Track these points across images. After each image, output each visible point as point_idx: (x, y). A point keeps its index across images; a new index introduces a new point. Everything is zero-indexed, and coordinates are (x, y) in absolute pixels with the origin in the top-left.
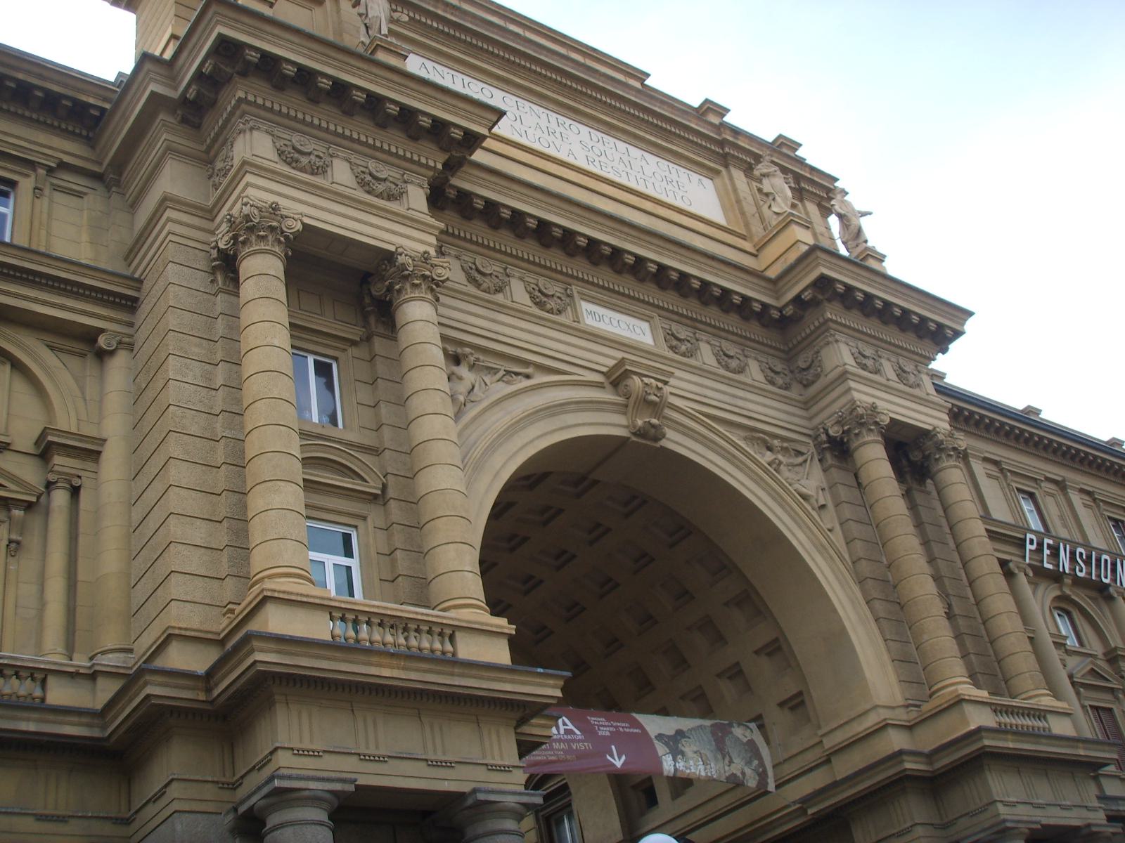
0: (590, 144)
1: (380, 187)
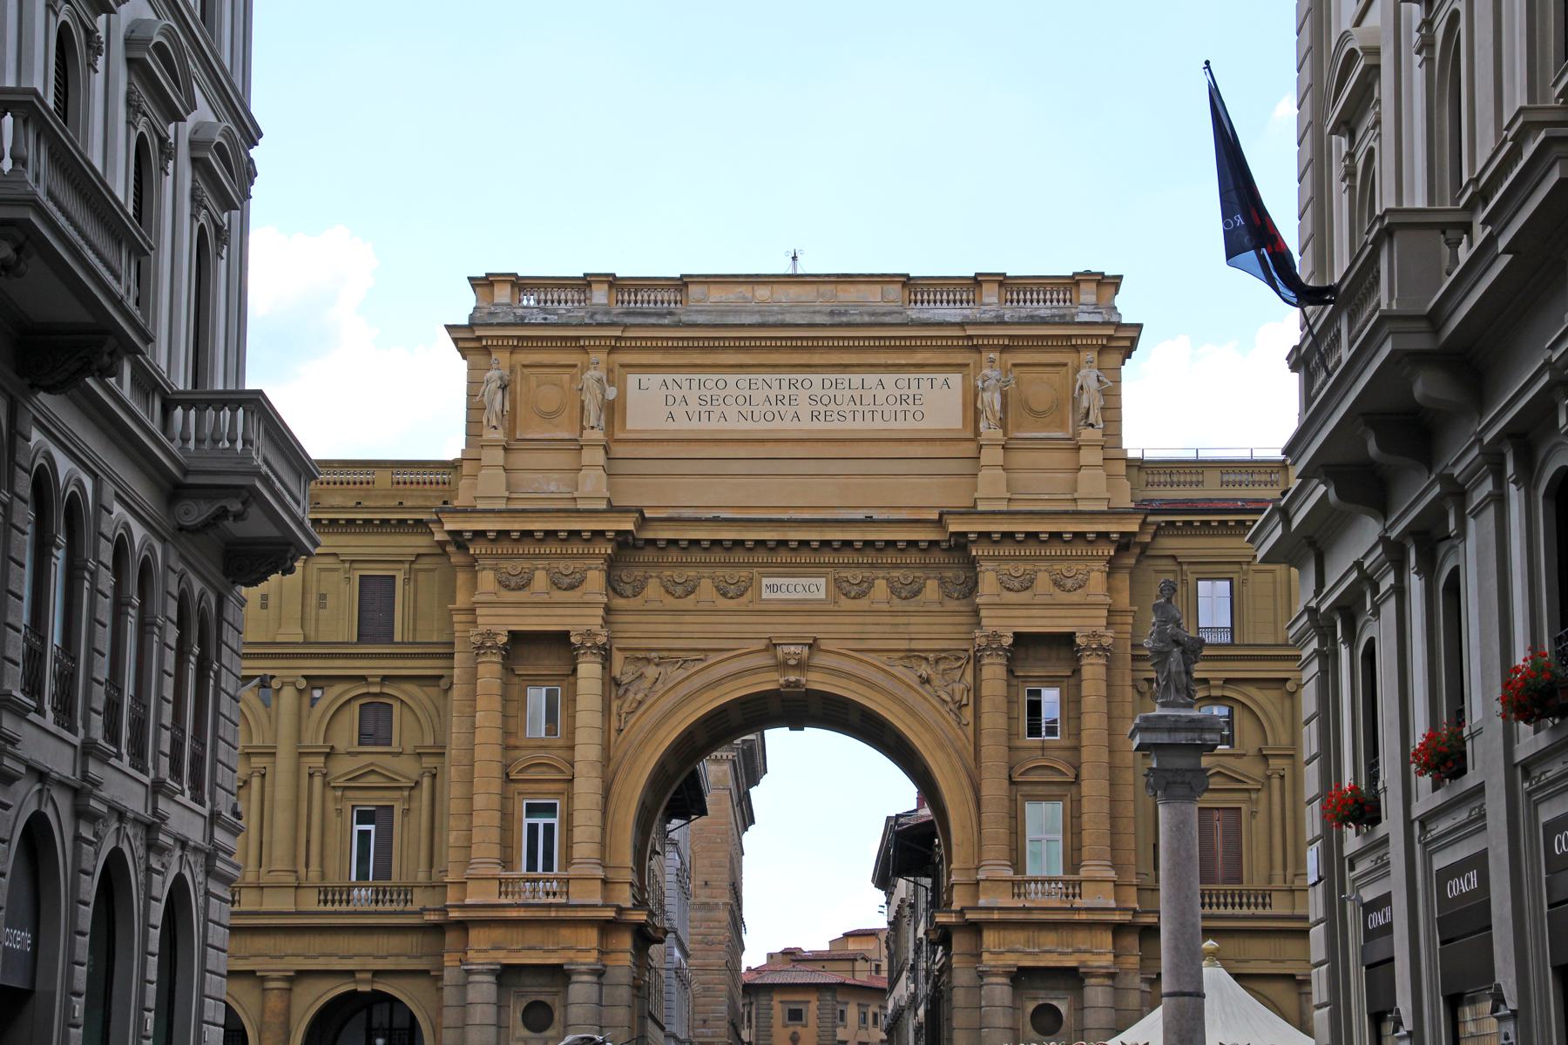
0: (820, 393)
1: (567, 580)
